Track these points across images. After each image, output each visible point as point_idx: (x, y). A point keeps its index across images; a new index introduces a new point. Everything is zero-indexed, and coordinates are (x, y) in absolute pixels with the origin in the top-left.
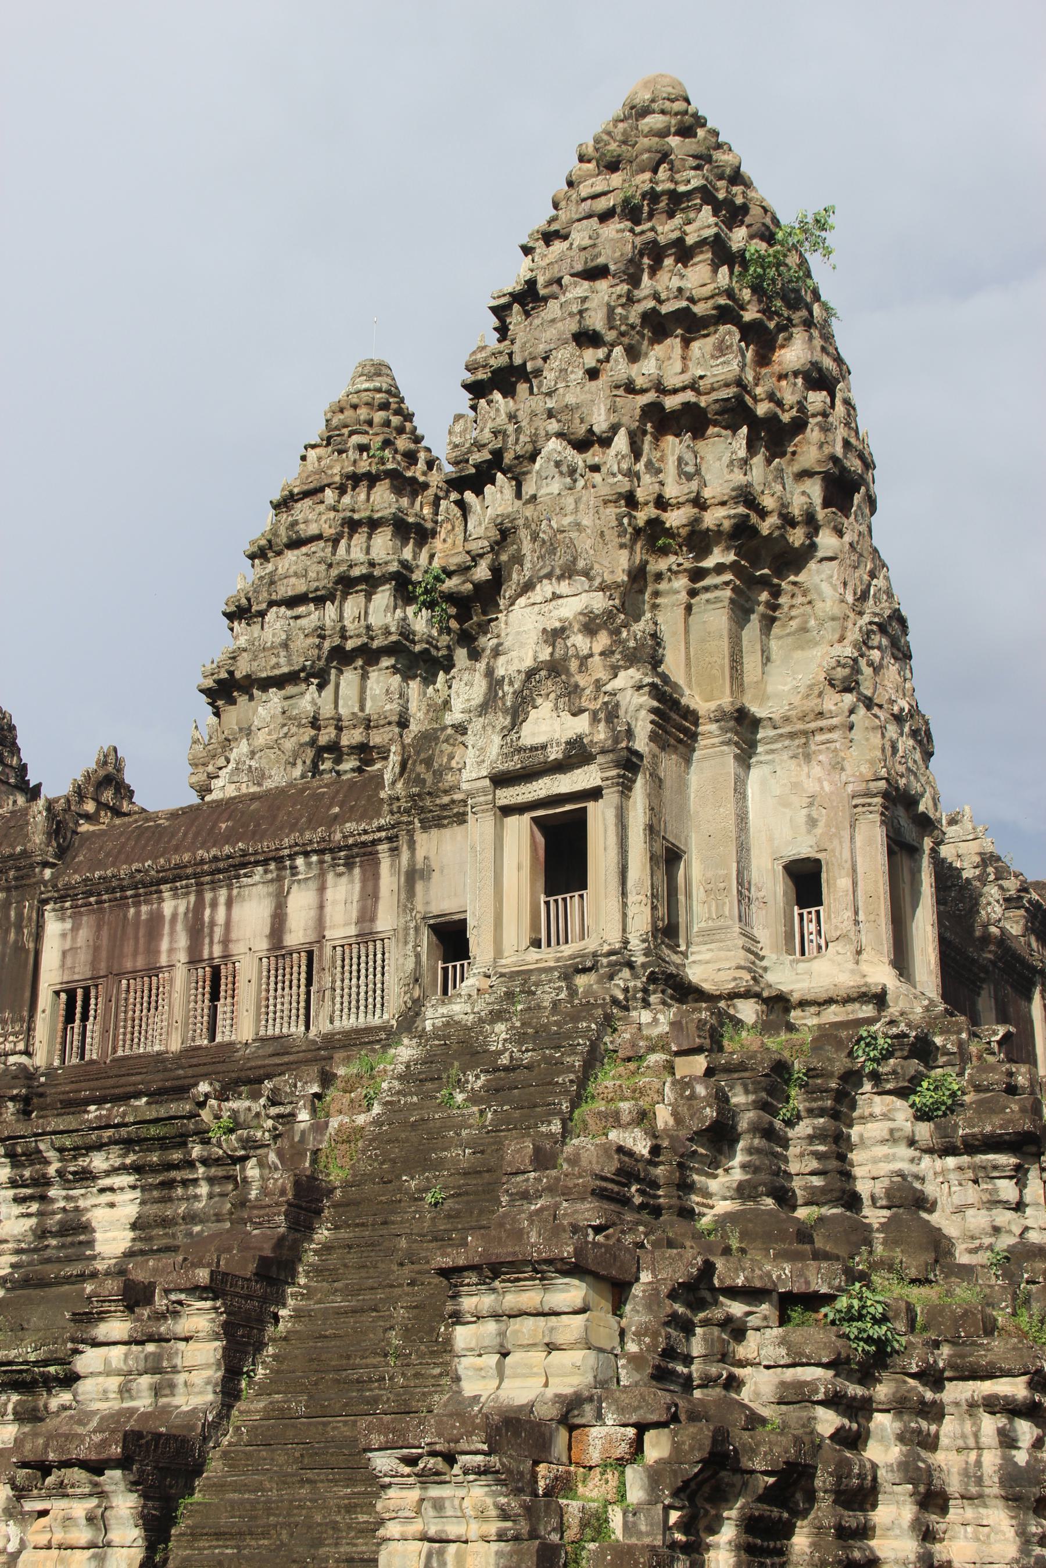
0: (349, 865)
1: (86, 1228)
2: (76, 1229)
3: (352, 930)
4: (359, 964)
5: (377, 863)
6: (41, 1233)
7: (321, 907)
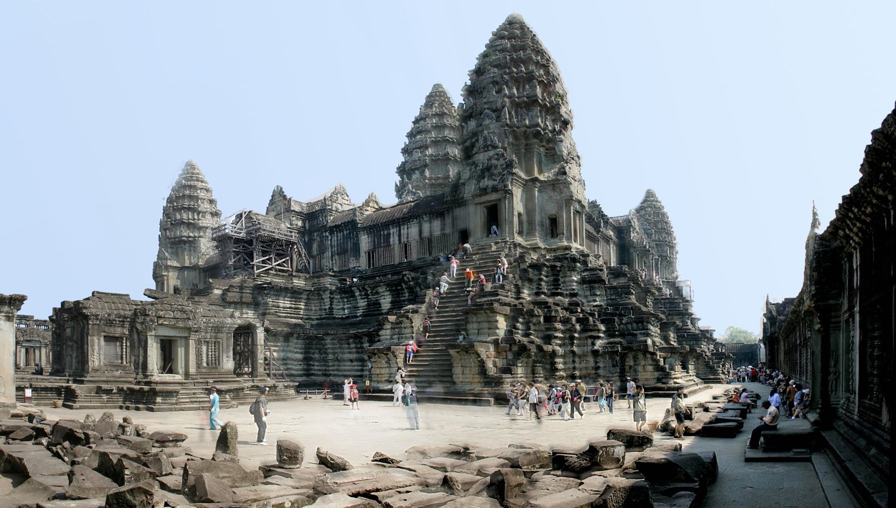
1: (380, 304)
2: (377, 304)
6: (368, 305)
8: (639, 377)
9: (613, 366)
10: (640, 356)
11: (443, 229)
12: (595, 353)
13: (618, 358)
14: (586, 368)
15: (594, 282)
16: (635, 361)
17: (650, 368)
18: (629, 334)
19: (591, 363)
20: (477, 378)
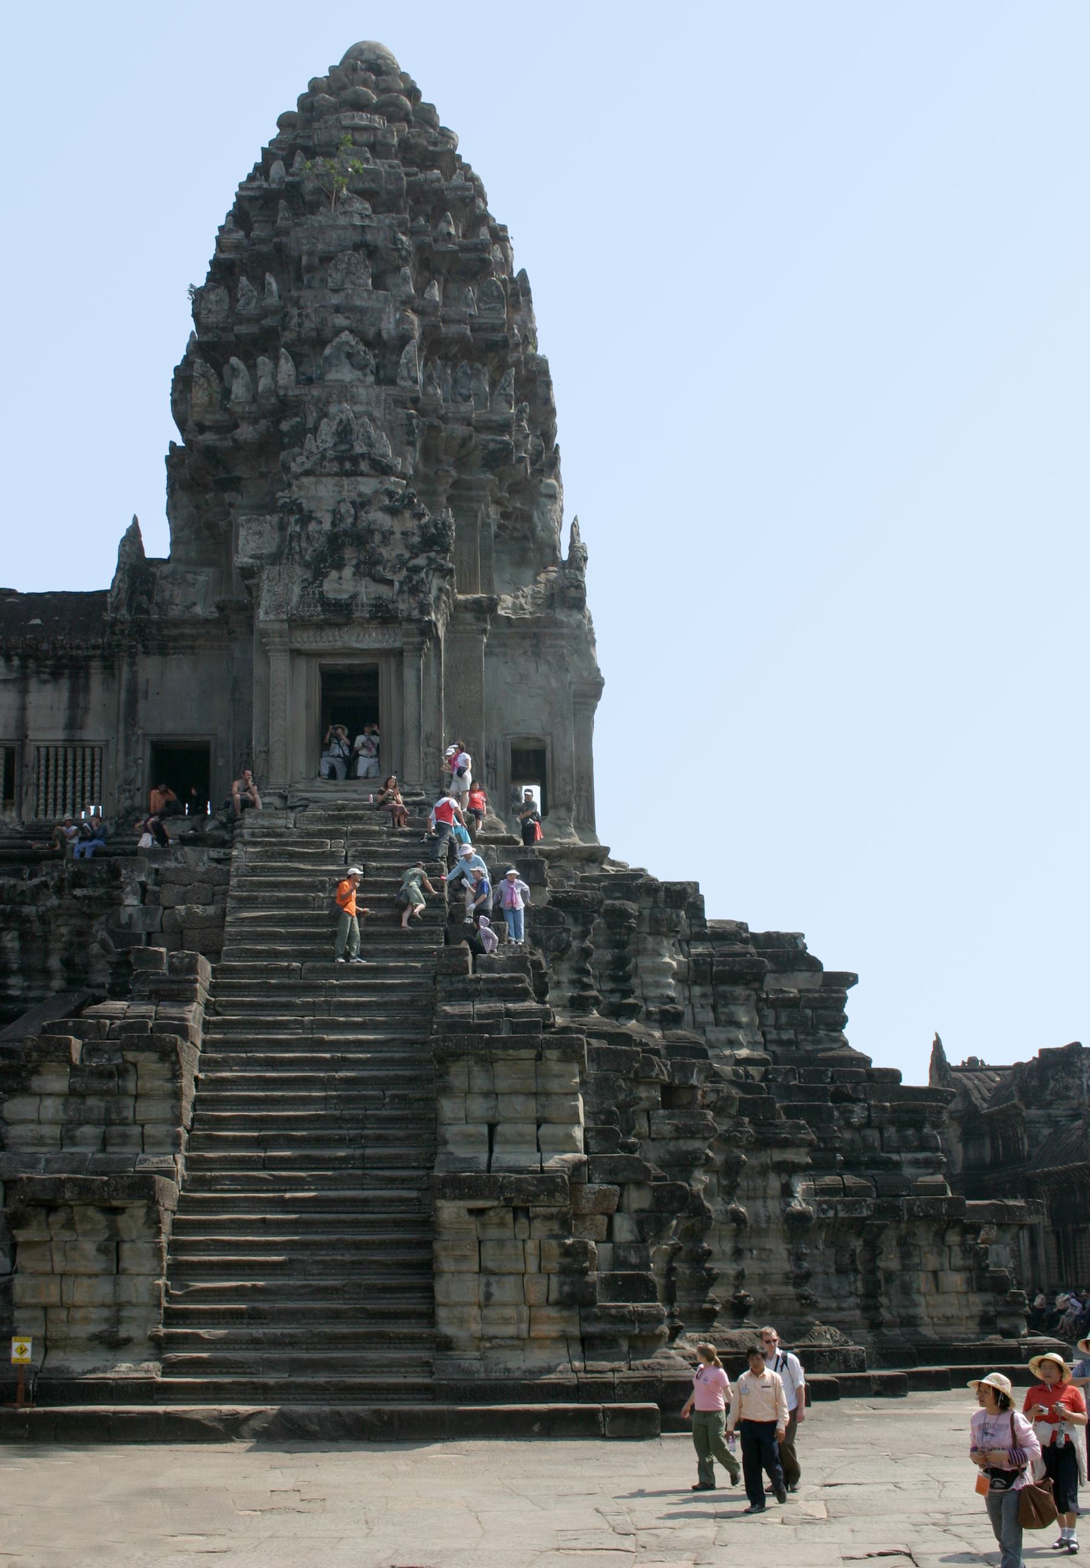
0: (56, 675)
3: (60, 735)
4: (47, 767)
5: (88, 676)
7: (23, 708)
8: (921, 1311)
9: (841, 1271)
10: (924, 1237)
11: (73, 724)
12: (796, 1223)
13: (857, 1244)
14: (764, 1278)
15: (735, 978)
16: (905, 1255)
17: (955, 1280)
18: (875, 1163)
19: (780, 1261)
20: (551, 1323)
